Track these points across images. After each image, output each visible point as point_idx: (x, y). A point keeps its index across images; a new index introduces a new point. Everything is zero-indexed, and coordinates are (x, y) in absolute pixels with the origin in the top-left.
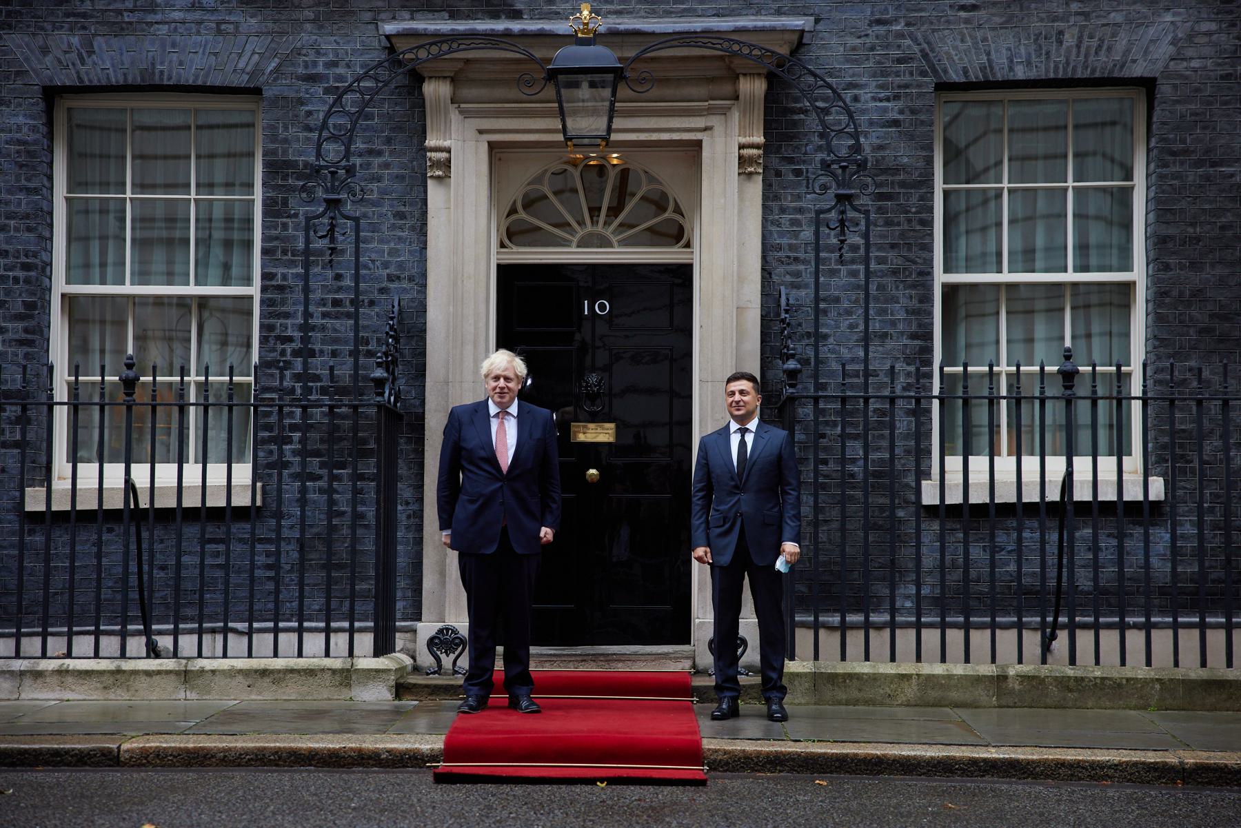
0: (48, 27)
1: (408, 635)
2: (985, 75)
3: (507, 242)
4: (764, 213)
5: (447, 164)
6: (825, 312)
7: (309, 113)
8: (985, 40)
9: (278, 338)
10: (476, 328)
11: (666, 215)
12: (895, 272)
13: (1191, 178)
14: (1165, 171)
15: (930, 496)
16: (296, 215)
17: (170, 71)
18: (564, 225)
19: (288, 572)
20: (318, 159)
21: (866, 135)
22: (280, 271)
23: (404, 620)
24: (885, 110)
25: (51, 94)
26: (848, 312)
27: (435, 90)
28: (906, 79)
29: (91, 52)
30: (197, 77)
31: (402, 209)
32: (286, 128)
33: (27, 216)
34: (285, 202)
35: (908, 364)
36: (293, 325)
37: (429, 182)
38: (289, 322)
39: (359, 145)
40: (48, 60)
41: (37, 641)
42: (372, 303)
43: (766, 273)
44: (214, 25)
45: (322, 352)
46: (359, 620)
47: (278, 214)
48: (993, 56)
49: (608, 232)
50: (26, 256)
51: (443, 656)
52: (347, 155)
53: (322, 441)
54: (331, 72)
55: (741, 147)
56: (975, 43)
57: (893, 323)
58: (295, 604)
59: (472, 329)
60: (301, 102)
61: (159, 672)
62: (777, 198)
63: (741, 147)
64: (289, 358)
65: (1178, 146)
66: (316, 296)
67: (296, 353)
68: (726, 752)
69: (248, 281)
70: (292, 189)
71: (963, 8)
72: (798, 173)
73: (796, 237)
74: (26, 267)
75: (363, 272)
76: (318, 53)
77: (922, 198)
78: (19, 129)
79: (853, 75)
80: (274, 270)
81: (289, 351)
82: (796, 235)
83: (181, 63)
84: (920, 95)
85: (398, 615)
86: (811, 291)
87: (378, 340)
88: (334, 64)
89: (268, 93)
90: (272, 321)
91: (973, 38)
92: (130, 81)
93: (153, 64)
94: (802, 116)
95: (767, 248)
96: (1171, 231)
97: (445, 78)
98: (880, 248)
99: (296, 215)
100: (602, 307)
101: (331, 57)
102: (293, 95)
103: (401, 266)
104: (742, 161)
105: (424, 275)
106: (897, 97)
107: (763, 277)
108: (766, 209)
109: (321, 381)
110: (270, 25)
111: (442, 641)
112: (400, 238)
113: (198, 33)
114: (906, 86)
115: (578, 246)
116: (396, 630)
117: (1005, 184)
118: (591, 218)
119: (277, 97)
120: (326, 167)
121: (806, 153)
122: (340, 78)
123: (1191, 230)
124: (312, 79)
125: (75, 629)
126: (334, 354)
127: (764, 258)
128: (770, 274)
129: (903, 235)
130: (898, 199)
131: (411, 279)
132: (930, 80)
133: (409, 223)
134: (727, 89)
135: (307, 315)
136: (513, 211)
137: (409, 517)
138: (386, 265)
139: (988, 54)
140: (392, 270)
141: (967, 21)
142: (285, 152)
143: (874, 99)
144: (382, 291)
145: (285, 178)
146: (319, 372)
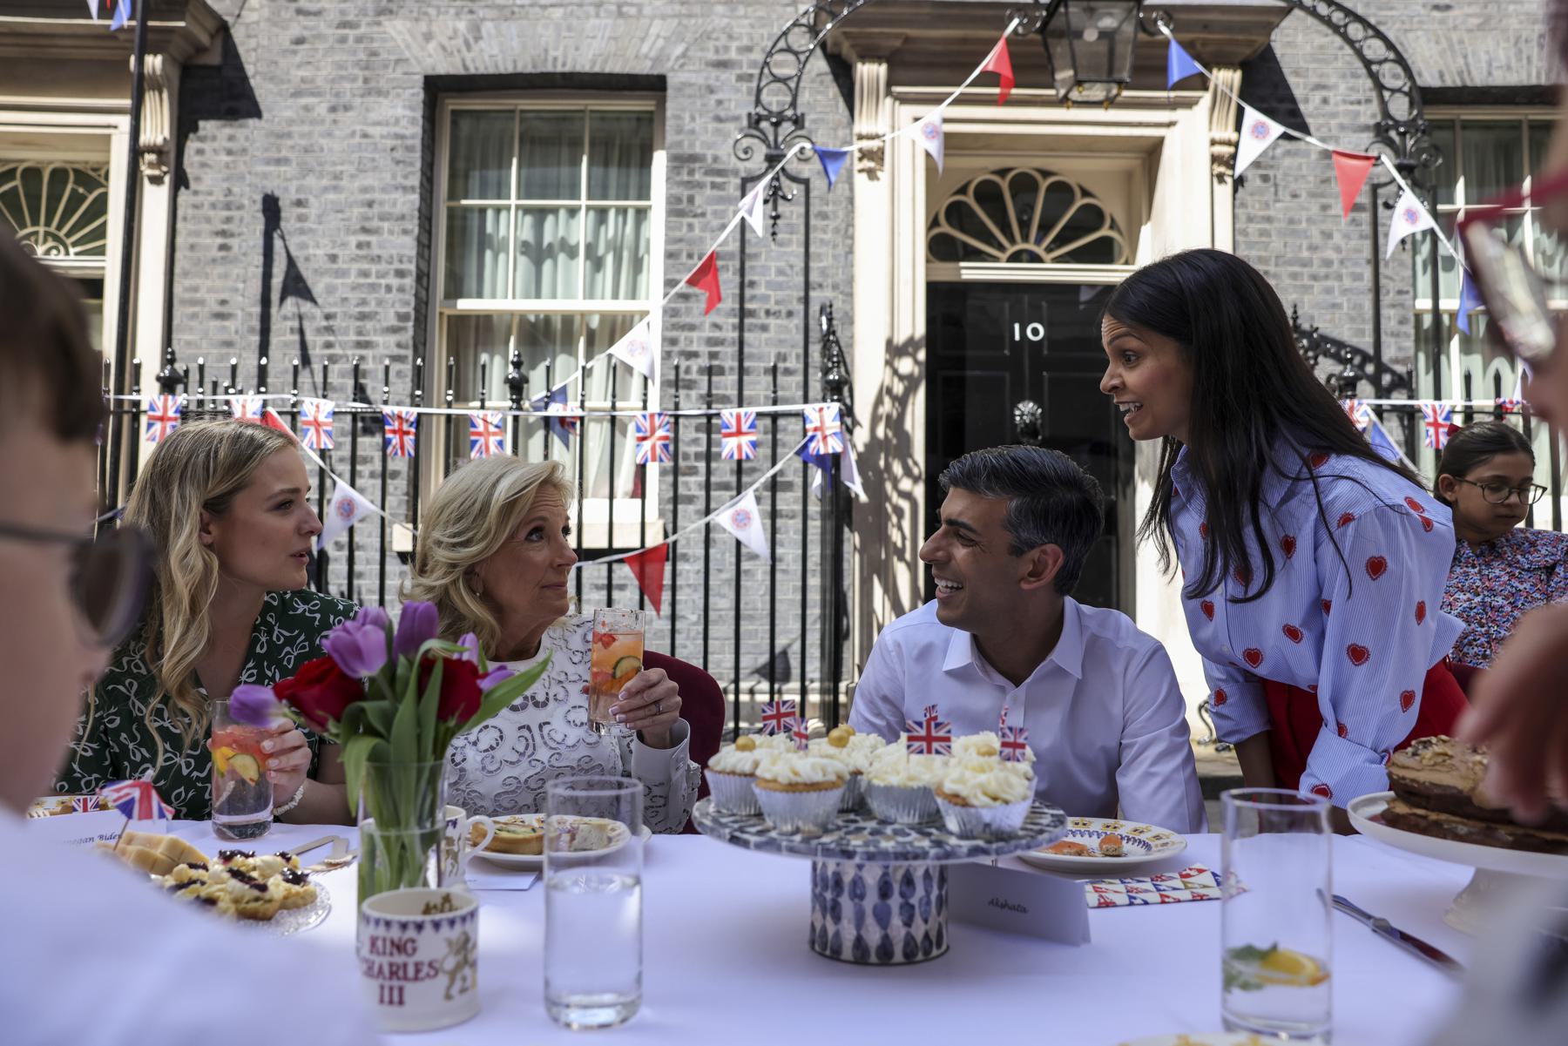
0: (432, 11)
2: (1462, 79)
5: (877, 156)
7: (720, 102)
8: (1461, 42)
16: (703, 215)
17: (565, 56)
18: (989, 239)
24: (1357, 114)
27: (870, 72)
29: (478, 38)
31: (825, 208)
32: (693, 119)
33: (403, 217)
34: (691, 200)
36: (699, 339)
37: (861, 180)
38: (695, 335)
40: (432, 46)
44: (614, 8)
48: (1470, 60)
49: (1040, 250)
50: (401, 261)
54: (745, 58)
56: (1451, 46)
60: (711, 90)
62: (1243, 205)
63: (1213, 143)
64: (694, 376)
67: (701, 371)
70: (700, 185)
71: (1437, 7)
72: (1265, 178)
74: (400, 274)
76: (730, 37)
78: (397, 121)
79: (1321, 76)
80: (677, 277)
81: (695, 369)
82: (1266, 246)
83: (577, 49)
88: (749, 49)
89: (673, 81)
90: (674, 334)
91: (1449, 40)
93: (546, 51)
98: (1356, 264)
99: (703, 215)
101: (745, 42)
104: (1215, 159)
105: (850, 281)
110: (677, 7)
112: (822, 241)
113: (597, 15)
121: (1273, 158)
124: (723, 65)
131: (835, 287)
133: (832, 224)
139: (1465, 57)
141: (1442, 22)
142: (692, 145)
143: (1345, 102)
145: (691, 172)
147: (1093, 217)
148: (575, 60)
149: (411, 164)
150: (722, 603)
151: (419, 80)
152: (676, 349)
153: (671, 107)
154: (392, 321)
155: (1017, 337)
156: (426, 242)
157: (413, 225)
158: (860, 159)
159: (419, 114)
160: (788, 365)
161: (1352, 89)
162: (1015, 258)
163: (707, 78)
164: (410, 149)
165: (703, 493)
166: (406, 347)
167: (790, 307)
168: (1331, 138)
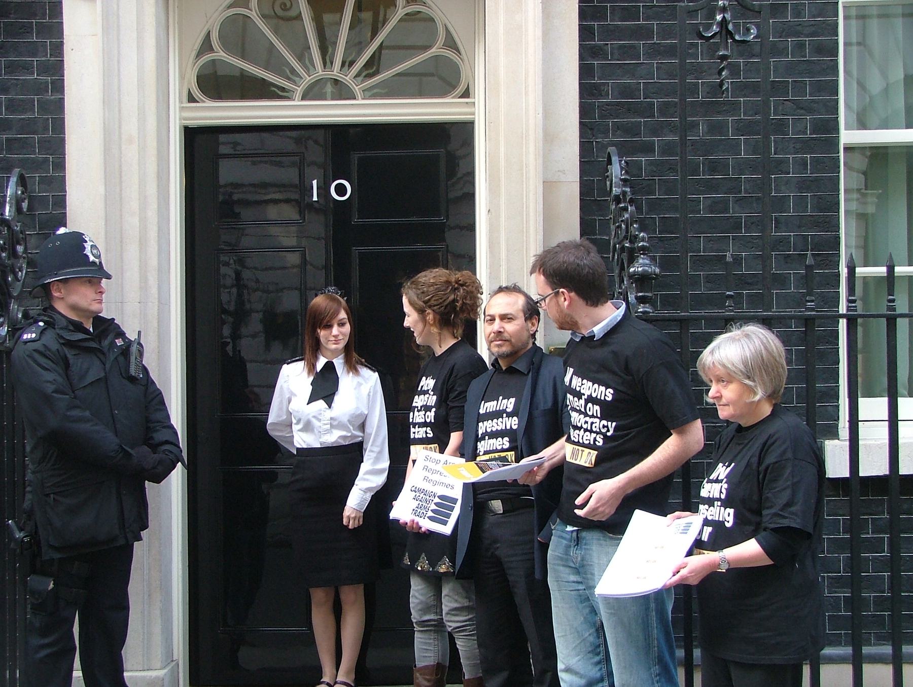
3: (197, 93)
4: (582, 38)
10: (143, 220)
11: (433, 51)
12: (780, 127)
15: (837, 465)
26: (711, 186)
43: (587, 128)
49: (348, 78)
57: (781, 203)
59: (135, 221)
73: (633, 76)
95: (588, 90)
100: (341, 190)
107: (582, 136)
108: (585, 32)
129: (790, 68)
136: (206, 46)
155: (315, 198)
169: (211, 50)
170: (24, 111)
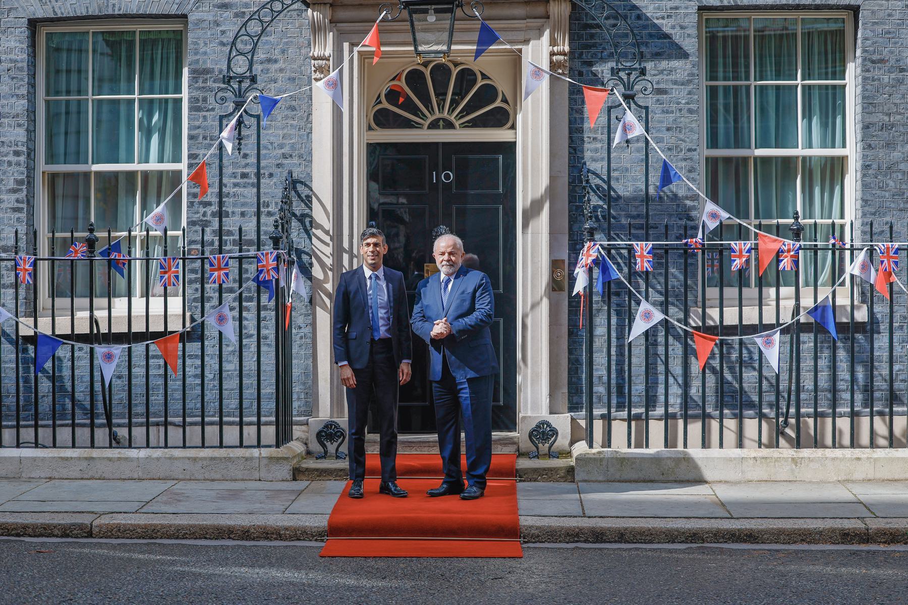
1: (304, 428)
3: (373, 125)
4: (570, 104)
6: (617, 179)
7: (223, 32)
9: (201, 203)
12: (669, 149)
13: (886, 80)
14: (867, 75)
19: (211, 380)
20: (228, 71)
21: (646, 44)
22: (202, 152)
23: (298, 416)
25: (34, 24)
28: (677, 3)
30: (140, 8)
31: (294, 103)
32: (206, 44)
33: (17, 115)
34: (205, 100)
35: (680, 219)
39: (260, 55)
41: (31, 431)
42: (271, 175)
45: (233, 213)
46: (265, 416)
47: (199, 109)
49: (452, 118)
50: (17, 145)
51: (328, 444)
52: (250, 69)
53: (235, 281)
55: (552, 54)
58: (217, 404)
61: (119, 459)
64: (208, 218)
65: (875, 57)
66: (228, 170)
67: (213, 214)
68: (538, 528)
69: (177, 159)
74: (17, 153)
75: (263, 152)
77: (690, 93)
84: (686, 15)
85: (295, 413)
86: (605, 163)
87: (276, 204)
89: (192, 18)
92: (90, 13)
94: (598, 30)
96: (873, 119)
97: (325, 4)
98: (659, 131)
99: (213, 109)
100: (447, 177)
102: (211, 18)
103: (293, 147)
105: (310, 153)
106: (669, 17)
107: (570, 153)
109: (233, 235)
111: (328, 433)
114: (677, 8)
115: (429, 128)
116: (292, 424)
117: (753, 83)
118: (438, 105)
119: (199, 20)
120: (235, 78)
122: (247, 5)
123: (886, 118)
124: (224, 6)
125: (58, 422)
126: (243, 214)
127: (571, 138)
128: (575, 150)
130: (671, 93)
131: (301, 156)
132: (693, 7)
133: (300, 113)
134: (540, 10)
135: (221, 185)
137: (301, 338)
138: (281, 146)
140: (286, 150)
142: (205, 62)
144: (279, 166)
145: (205, 81)
146: (231, 229)
147: (489, 93)
148: (127, 6)
149: (22, 79)
150: (231, 367)
151: (25, 21)
152: (197, 200)
153: (191, 37)
154: (11, 185)
156: (32, 128)
157: (23, 120)
158: (315, 71)
159: (25, 46)
160: (270, 209)
161: (658, 8)
162: (434, 125)
163: (215, 16)
164: (21, 69)
165: (217, 294)
166: (22, 202)
167: (271, 171)
168: (643, 43)
169: (380, 102)
170: (291, 139)
